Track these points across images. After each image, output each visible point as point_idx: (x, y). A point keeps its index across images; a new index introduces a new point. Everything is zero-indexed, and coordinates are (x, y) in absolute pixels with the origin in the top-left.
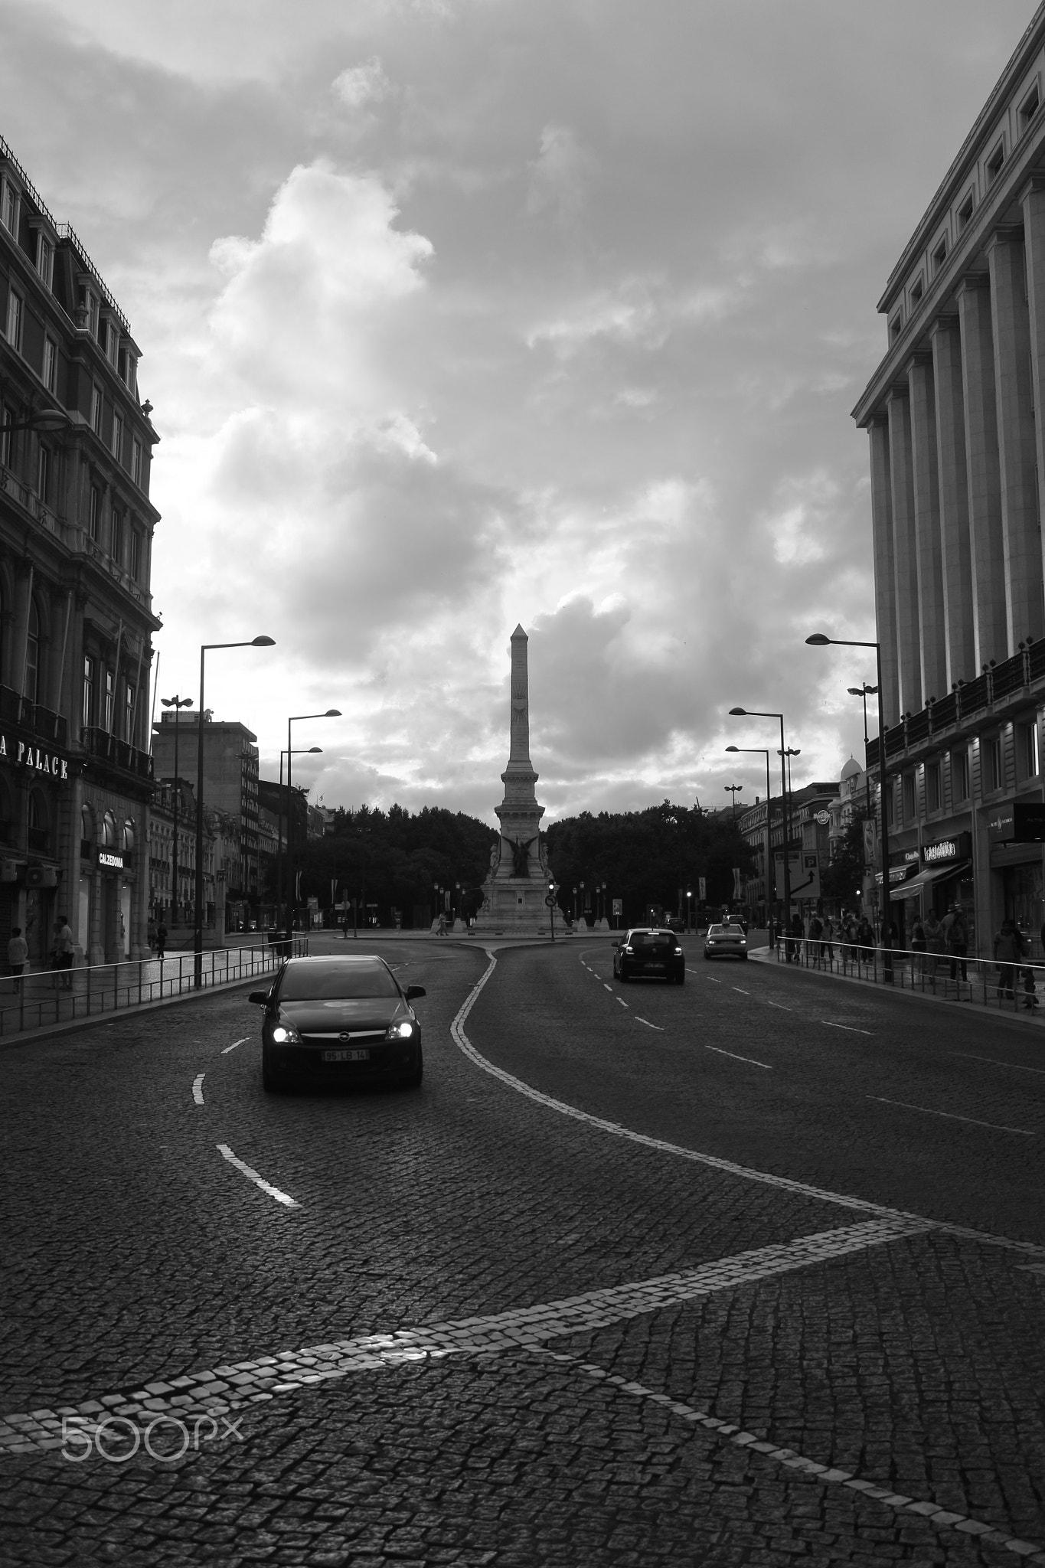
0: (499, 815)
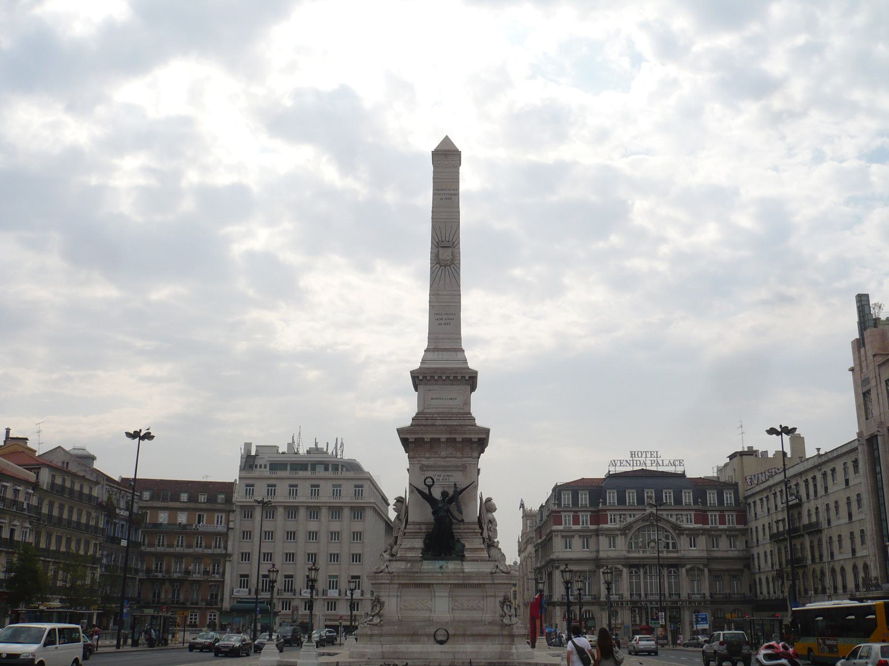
0: (405, 442)
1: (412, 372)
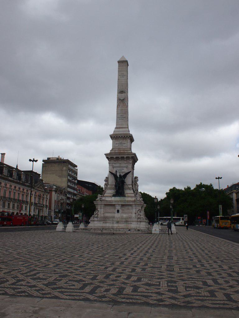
0: (107, 158)
1: (110, 135)
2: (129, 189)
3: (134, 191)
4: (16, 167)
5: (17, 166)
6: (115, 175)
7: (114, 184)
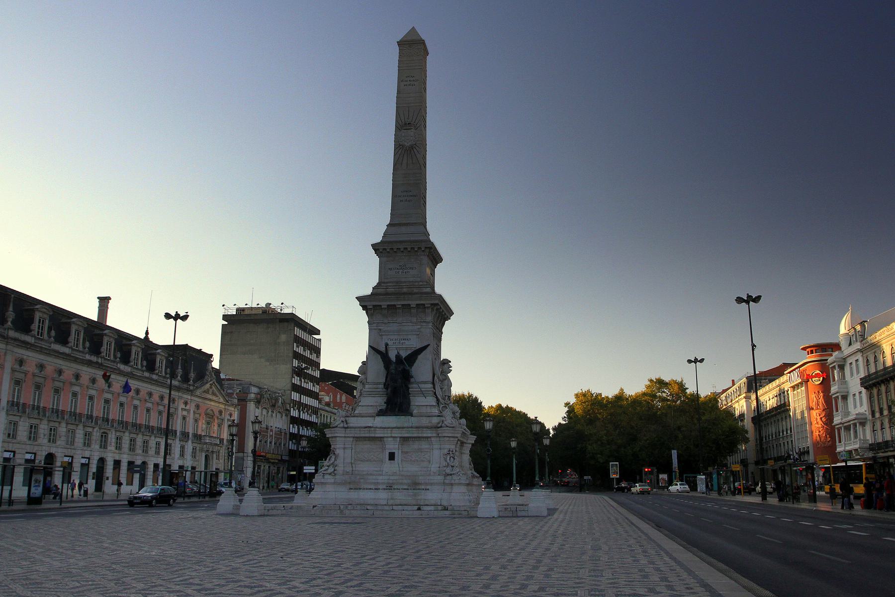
0: (364, 308)
1: (372, 245)
2: (423, 394)
3: (438, 400)
4: (142, 336)
5: (147, 333)
6: (384, 356)
7: (384, 380)
